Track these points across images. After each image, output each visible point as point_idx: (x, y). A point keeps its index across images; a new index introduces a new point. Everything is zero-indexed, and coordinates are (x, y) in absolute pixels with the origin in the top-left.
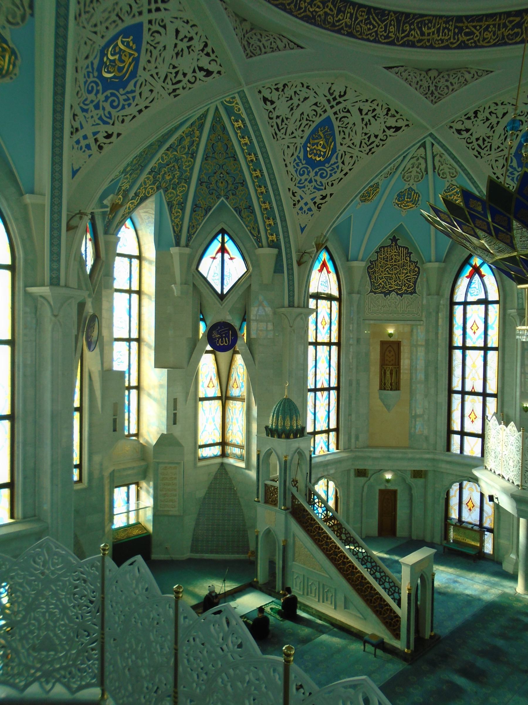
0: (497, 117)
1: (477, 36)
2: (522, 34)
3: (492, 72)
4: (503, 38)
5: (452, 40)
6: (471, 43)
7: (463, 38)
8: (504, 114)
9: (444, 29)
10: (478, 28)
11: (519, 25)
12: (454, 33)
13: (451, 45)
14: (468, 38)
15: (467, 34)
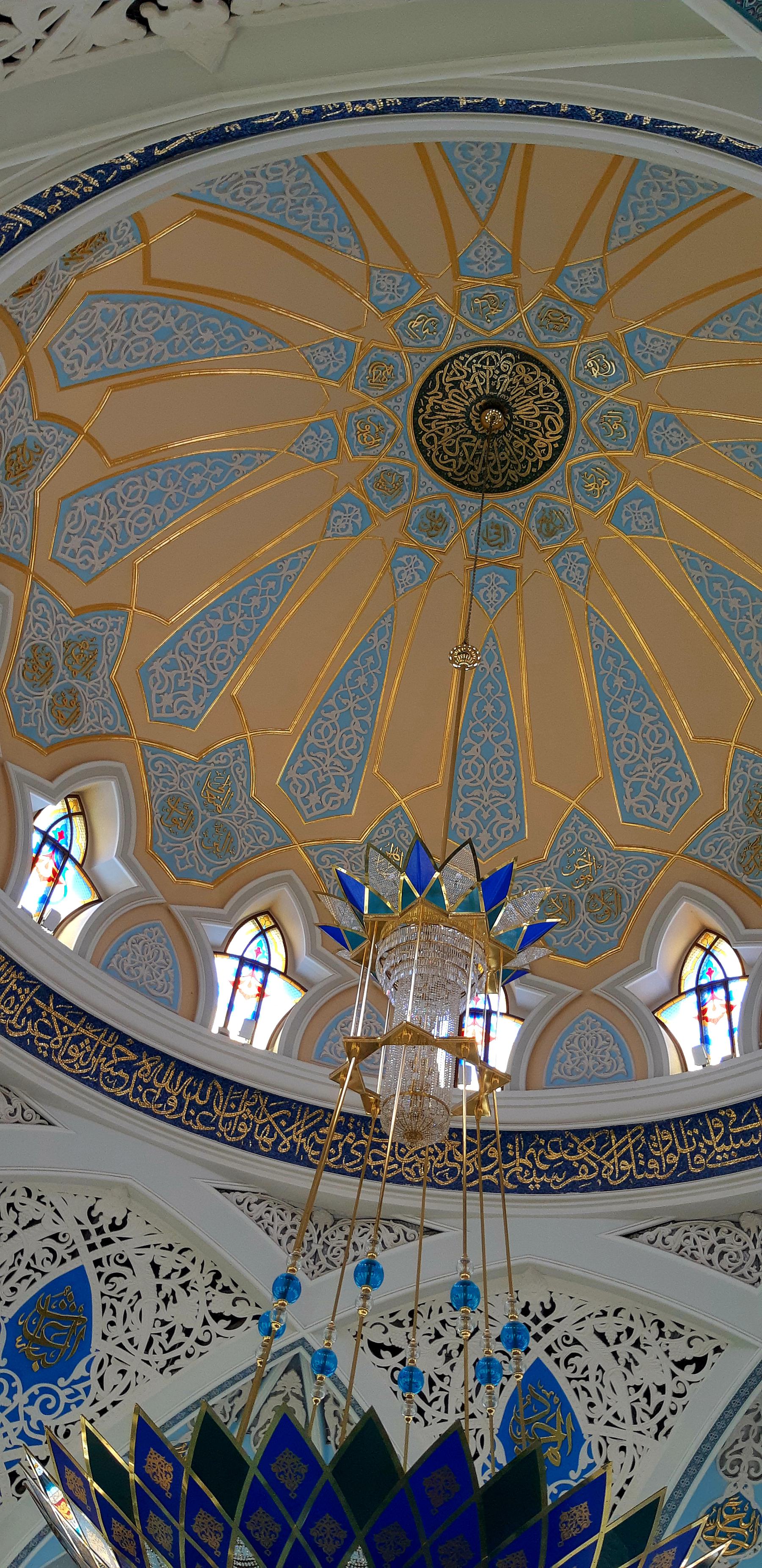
0: (17, 1222)
1: (57, 1042)
2: (128, 1086)
3: (50, 1124)
4: (96, 1075)
5: (14, 1021)
6: (43, 1048)
7: (32, 1029)
8: (33, 1223)
9: (12, 992)
10: (65, 1028)
11: (129, 1067)
12: (24, 1012)
13: (8, 1031)
14: (42, 1035)
15: (43, 1028)
